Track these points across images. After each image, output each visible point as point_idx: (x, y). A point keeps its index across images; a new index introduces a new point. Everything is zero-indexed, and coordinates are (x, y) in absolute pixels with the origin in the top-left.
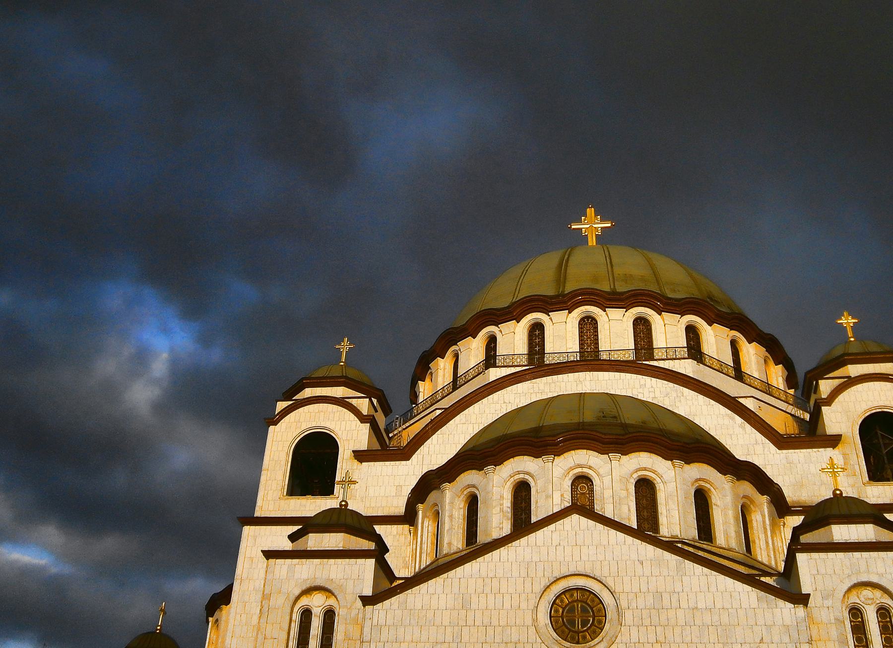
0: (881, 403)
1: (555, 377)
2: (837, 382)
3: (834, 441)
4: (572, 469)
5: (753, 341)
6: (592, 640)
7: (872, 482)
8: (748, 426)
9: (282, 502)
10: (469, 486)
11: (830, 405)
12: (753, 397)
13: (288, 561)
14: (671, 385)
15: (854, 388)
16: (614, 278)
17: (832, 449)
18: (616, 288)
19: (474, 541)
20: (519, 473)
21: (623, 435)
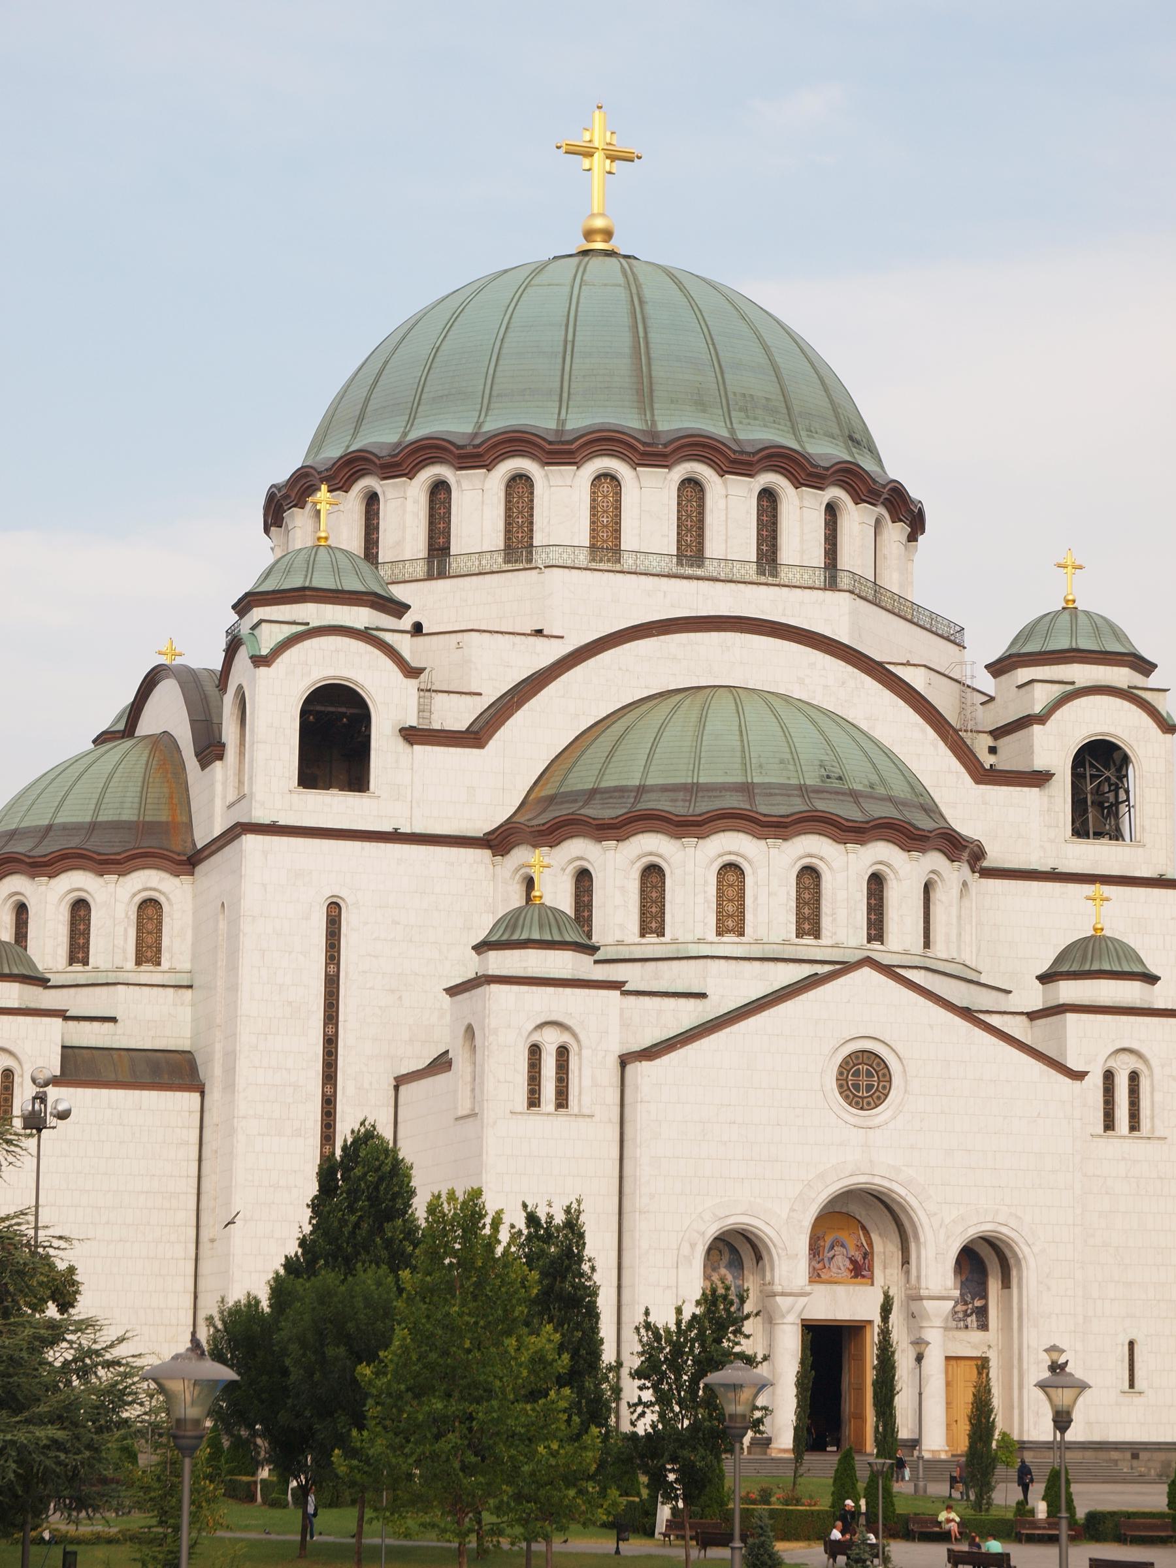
0: (1105, 729)
1: (692, 635)
2: (1057, 691)
3: (1039, 779)
4: (801, 858)
5: (901, 521)
6: (877, 1106)
7: (1075, 839)
8: (941, 744)
9: (295, 796)
10: (651, 854)
11: (1044, 724)
12: (925, 666)
13: (515, 988)
14: (850, 668)
15: (1077, 702)
16: (728, 404)
17: (1035, 791)
18: (735, 426)
19: (654, 925)
20: (730, 853)
21: (867, 822)
